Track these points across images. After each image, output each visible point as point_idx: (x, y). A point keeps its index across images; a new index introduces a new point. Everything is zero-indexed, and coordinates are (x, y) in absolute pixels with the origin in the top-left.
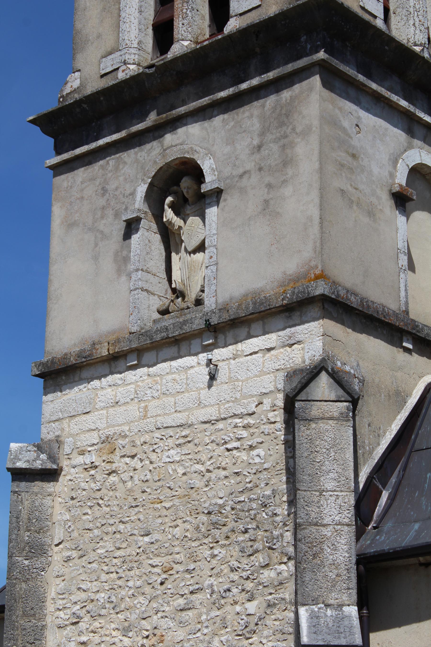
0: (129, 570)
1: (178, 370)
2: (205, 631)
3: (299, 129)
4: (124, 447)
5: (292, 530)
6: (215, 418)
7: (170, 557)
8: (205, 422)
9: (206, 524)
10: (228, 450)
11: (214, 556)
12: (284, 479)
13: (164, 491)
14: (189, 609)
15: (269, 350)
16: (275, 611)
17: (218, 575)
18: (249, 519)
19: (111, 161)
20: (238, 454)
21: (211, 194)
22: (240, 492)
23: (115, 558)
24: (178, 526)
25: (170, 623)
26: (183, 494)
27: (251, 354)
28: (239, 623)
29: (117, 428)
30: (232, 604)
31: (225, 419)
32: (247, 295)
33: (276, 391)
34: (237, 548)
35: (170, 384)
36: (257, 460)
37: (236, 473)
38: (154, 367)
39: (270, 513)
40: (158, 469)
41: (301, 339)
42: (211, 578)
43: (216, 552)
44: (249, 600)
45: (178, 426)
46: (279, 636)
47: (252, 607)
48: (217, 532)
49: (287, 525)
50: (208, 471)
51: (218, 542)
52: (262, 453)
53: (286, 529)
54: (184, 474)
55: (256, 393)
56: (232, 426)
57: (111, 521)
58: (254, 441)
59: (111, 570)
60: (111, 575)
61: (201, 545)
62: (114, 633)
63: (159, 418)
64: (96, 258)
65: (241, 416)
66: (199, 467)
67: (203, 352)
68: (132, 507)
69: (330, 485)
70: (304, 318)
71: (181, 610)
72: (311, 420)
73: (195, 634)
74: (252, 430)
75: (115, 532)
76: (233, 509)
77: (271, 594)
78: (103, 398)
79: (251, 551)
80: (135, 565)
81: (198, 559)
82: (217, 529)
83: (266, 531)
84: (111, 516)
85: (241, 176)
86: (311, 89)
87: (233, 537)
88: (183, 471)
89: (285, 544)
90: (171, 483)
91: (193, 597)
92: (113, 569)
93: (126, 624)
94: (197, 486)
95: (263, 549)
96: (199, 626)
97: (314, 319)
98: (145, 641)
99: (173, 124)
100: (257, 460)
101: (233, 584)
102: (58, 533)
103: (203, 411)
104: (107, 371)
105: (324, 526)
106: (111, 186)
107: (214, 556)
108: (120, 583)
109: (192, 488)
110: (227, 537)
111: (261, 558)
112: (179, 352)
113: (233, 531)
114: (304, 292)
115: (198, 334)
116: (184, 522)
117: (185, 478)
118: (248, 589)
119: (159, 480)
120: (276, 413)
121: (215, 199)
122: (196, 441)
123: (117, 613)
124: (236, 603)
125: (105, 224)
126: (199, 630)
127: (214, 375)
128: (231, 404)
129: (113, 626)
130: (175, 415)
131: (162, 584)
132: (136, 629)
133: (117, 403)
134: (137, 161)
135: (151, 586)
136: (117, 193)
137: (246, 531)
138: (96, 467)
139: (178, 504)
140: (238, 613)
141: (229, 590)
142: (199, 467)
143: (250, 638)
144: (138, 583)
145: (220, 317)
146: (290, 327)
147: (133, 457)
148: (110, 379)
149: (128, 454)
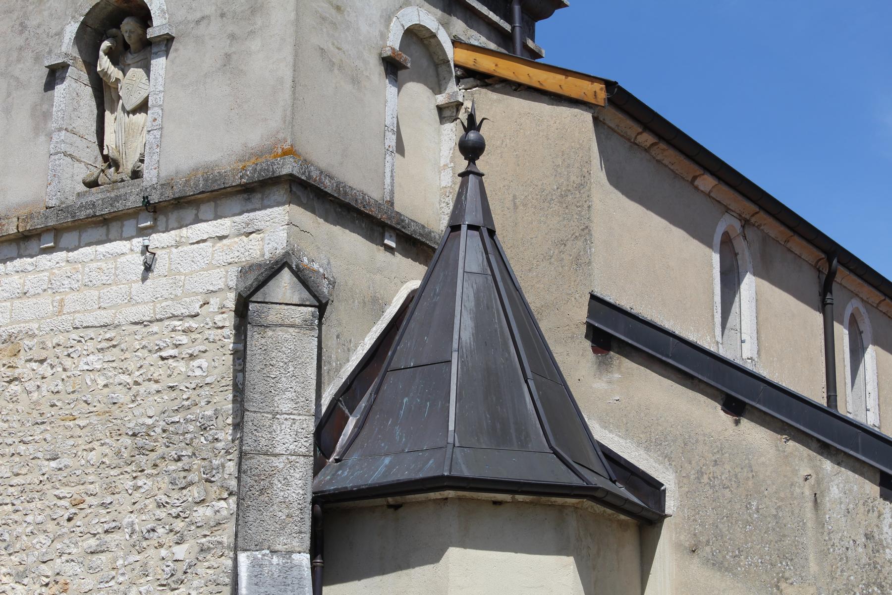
0: (28, 502)
2: (121, 579)
4: (30, 349)
5: (236, 460)
6: (148, 319)
7: (81, 487)
8: (136, 323)
9: (129, 448)
10: (163, 359)
11: (137, 488)
12: (231, 397)
13: (80, 406)
14: (102, 552)
15: (221, 238)
16: (209, 557)
17: (141, 511)
18: (183, 444)
20: (175, 364)
21: (160, 41)
22: (174, 411)
23: (12, 486)
24: (94, 449)
25: (77, 568)
26: (103, 410)
27: (198, 242)
28: (163, 571)
29: (22, 325)
30: (156, 548)
31: (161, 320)
32: (197, 169)
33: (227, 289)
34: (167, 479)
35: (94, 274)
36: (198, 372)
37: (171, 387)
38: (76, 252)
39: (210, 438)
40: (73, 378)
41: (261, 227)
42: (132, 515)
43: (140, 483)
44: (177, 543)
45: (101, 326)
47: (180, 551)
48: (143, 459)
49: (230, 454)
50: (136, 383)
51: (143, 471)
53: (228, 457)
54: (106, 386)
55: (201, 290)
56: (170, 329)
57: (10, 441)
58: (195, 350)
59: (5, 502)
60: (5, 507)
61: (122, 474)
62: (5, 580)
63: (77, 315)
65: (181, 318)
66: (125, 378)
67: (138, 236)
68: (37, 423)
69: (286, 406)
70: (266, 202)
71: (92, 553)
72: (267, 327)
73: (107, 582)
74: (193, 336)
75: (13, 454)
76: (164, 431)
77: (205, 536)
80: (37, 495)
81: (117, 490)
82: (143, 454)
83: (204, 459)
84: (10, 434)
85: (198, 22)
87: (162, 465)
88: (105, 382)
89: (226, 477)
90: (89, 396)
92: (8, 500)
93: (21, 568)
94: (121, 401)
95: (199, 481)
96: (113, 573)
97: (279, 204)
98: (44, 589)
100: (198, 372)
101: (159, 522)
103: (134, 309)
104: (15, 254)
105: (276, 455)
106: (32, 22)
107: (137, 488)
108: (15, 517)
109: (114, 403)
110: (156, 465)
111: (195, 493)
112: (107, 235)
113: (164, 458)
114: (268, 170)
115: (133, 214)
116: (102, 445)
117: (106, 390)
118: (178, 529)
119: (73, 392)
120: (225, 316)
121: (163, 48)
122: (123, 346)
123: (10, 554)
124: (161, 546)
125: (22, 69)
126: (113, 578)
127: (150, 266)
128: (169, 303)
129: (4, 570)
130: (98, 312)
131: (69, 520)
132: (33, 575)
133: (25, 293)
135: (56, 522)
136: (40, 31)
137: (179, 459)
139: (96, 422)
140: (163, 559)
141: (153, 530)
142: (125, 378)
143: (176, 589)
144: (40, 519)
145: (162, 194)
146: (248, 211)
147: (42, 362)
148: (18, 263)
149: (36, 358)
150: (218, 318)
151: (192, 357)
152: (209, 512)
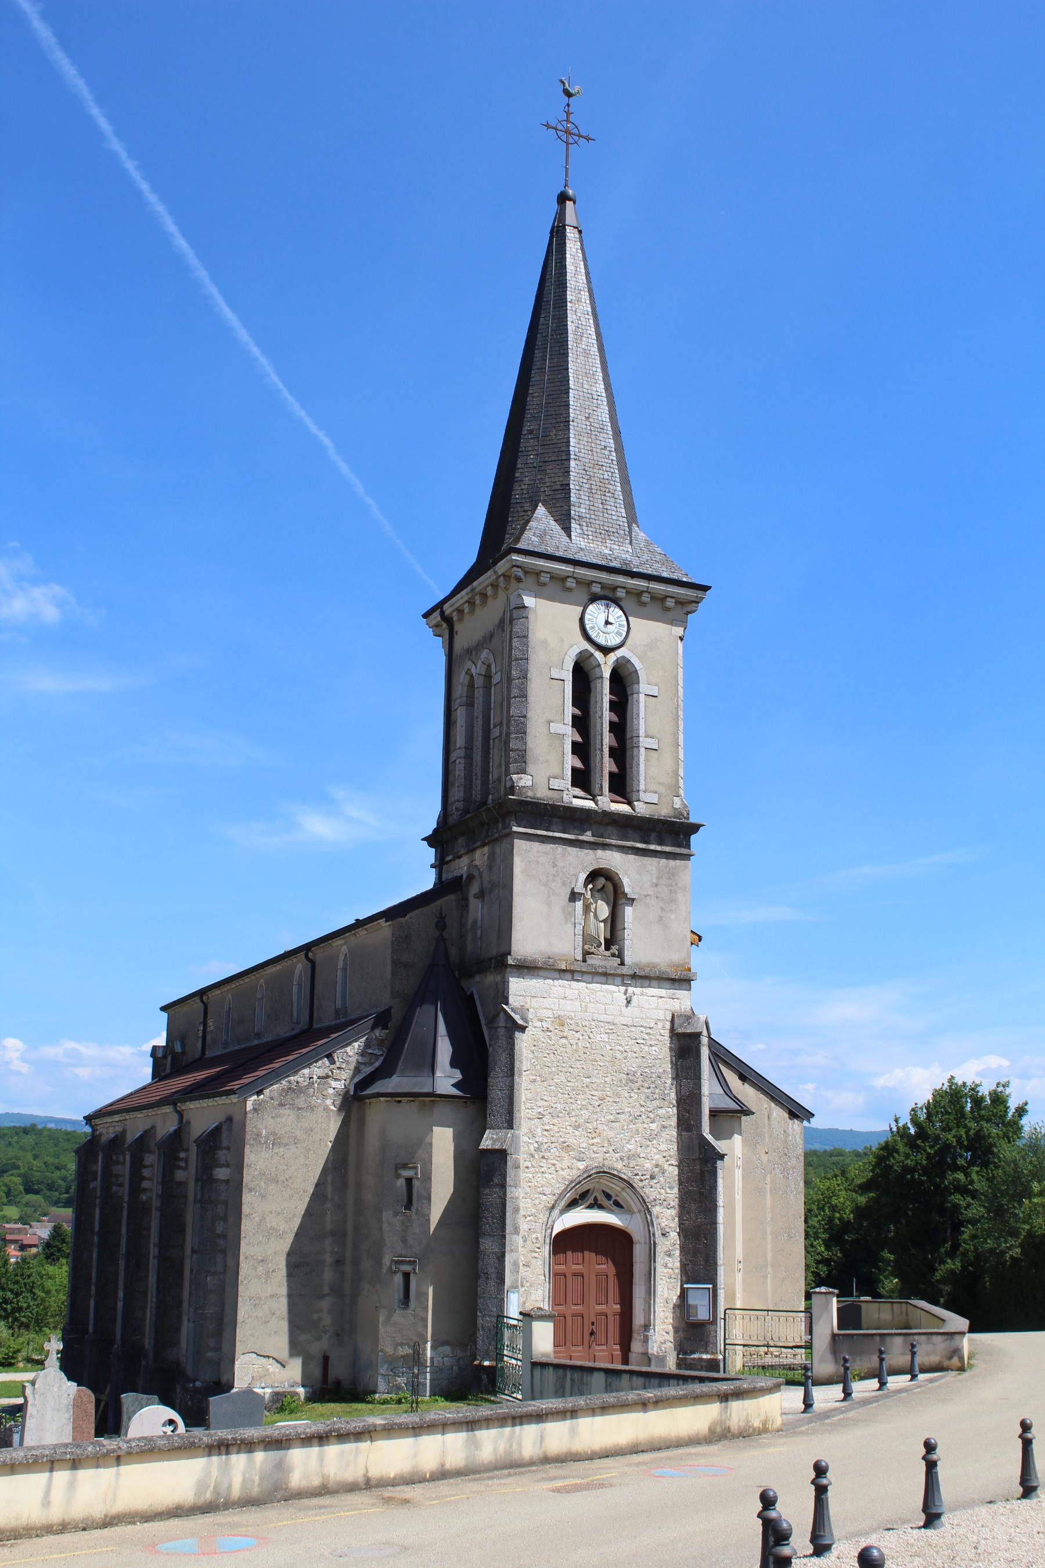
1: (606, 991)
19: (560, 848)
47: (653, 1126)
48: (633, 1086)
58: (653, 1043)
65: (646, 1027)
85: (646, 896)
99: (605, 846)
106: (560, 864)
111: (656, 1103)
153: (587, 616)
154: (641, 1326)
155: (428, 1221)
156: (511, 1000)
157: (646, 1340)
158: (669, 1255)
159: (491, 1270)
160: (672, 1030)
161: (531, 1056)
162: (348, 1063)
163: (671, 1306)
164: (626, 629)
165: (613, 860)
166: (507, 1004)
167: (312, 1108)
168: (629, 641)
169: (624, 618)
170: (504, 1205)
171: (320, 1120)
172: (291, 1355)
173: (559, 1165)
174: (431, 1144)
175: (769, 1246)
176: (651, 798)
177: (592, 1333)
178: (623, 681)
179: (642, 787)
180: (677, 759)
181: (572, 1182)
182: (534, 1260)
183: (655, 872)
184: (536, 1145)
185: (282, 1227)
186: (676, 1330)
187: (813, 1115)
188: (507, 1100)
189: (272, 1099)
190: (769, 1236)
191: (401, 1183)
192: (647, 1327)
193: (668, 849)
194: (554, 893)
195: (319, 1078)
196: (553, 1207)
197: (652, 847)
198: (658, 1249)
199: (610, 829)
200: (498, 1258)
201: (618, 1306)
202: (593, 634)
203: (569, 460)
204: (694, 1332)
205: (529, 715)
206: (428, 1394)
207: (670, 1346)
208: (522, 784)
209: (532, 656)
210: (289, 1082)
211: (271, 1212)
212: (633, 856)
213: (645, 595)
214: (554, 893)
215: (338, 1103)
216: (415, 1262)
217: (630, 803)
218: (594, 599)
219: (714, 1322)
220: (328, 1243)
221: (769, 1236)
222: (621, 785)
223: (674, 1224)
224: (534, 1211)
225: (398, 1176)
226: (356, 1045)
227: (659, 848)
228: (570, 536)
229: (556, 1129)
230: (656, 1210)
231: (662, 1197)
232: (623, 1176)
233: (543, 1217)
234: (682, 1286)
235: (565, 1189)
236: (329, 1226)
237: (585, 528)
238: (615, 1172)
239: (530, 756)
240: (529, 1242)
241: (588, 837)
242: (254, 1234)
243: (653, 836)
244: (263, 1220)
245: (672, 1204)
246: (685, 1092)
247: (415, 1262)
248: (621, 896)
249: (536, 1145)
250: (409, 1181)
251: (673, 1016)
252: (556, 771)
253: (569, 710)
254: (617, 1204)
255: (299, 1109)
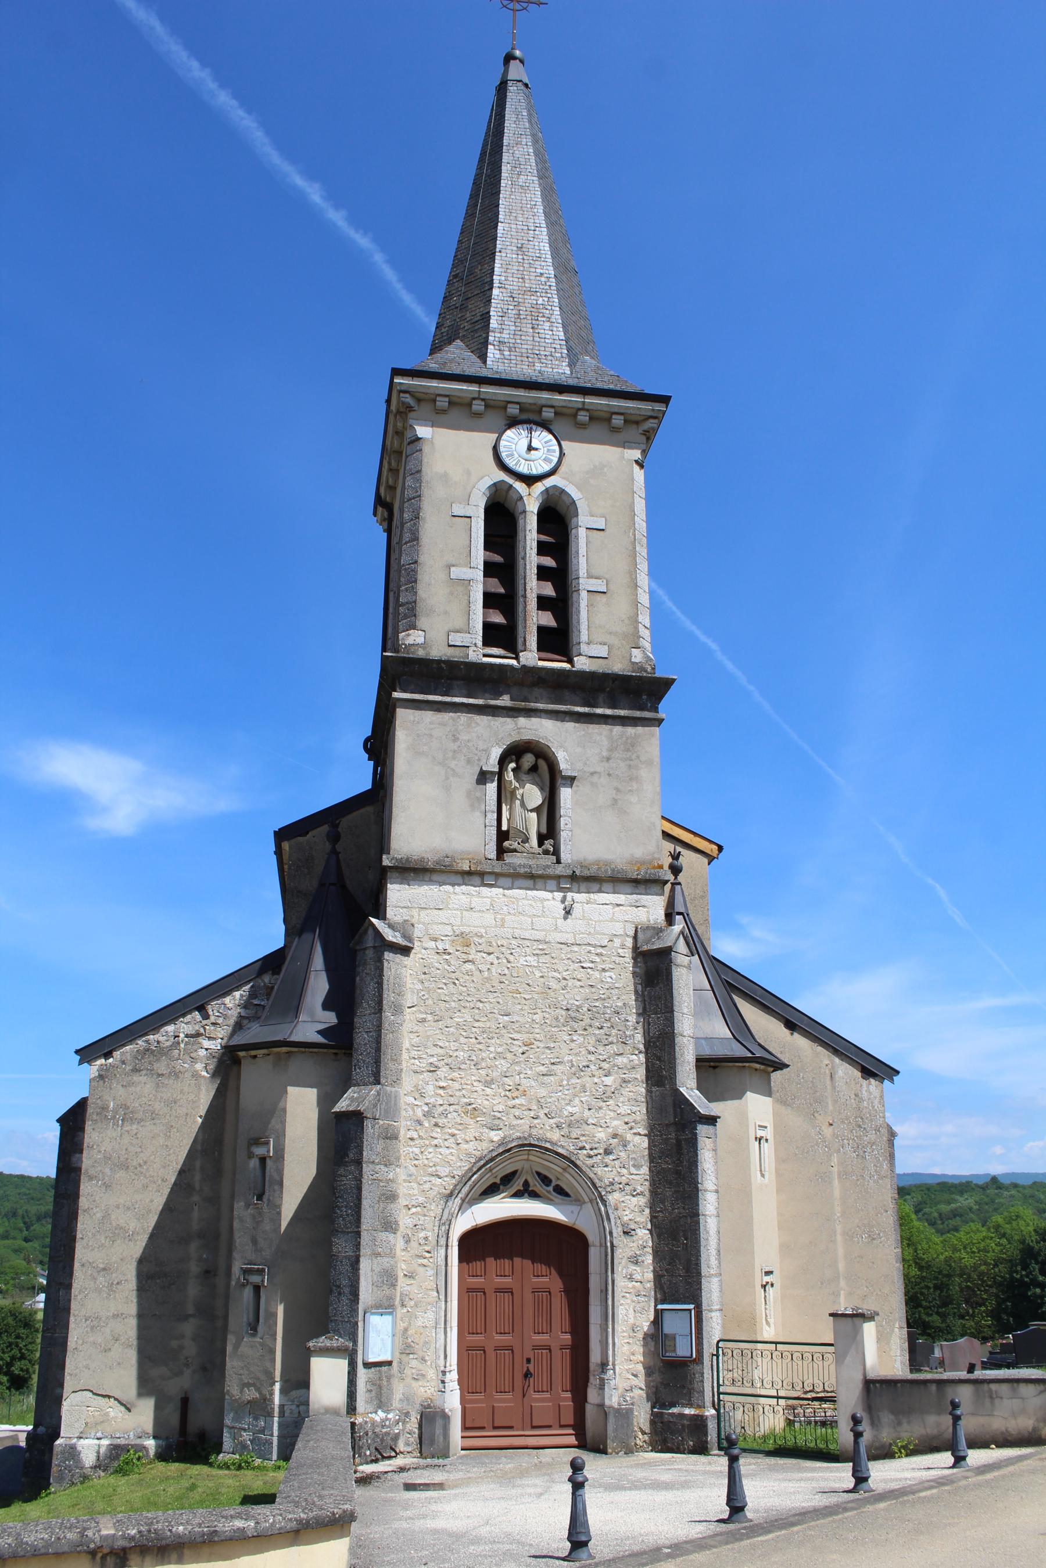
3: (643, 759)
11: (573, 1041)
15: (618, 905)
17: (577, 1054)
19: (463, 718)
36: (609, 980)
46: (633, 1103)
47: (608, 1080)
48: (575, 1025)
50: (565, 979)
52: (614, 977)
57: (469, 999)
58: (607, 966)
62: (475, 1084)
64: (447, 789)
65: (595, 946)
66: (556, 974)
69: (685, 1011)
78: (456, 901)
79: (606, 1042)
85: (592, 774)
86: (652, 735)
91: (554, 1067)
97: (657, 894)
99: (530, 713)
100: (609, 980)
102: (409, 999)
106: (464, 737)
107: (573, 1041)
108: (480, 1046)
115: (558, 878)
129: (473, 1078)
131: (523, 1053)
134: (489, 726)
137: (602, 1028)
138: (450, 954)
142: (556, 974)
144: (499, 1050)
147: (489, 954)
148: (463, 887)
150: (620, 951)
151: (603, 969)
152: (625, 1060)
153: (502, 443)
154: (597, 1365)
155: (279, 1214)
156: (390, 913)
157: (602, 1387)
158: (636, 1263)
159: (345, 1282)
160: (635, 948)
161: (420, 986)
162: (225, 1017)
163: (640, 1336)
164: (557, 454)
165: (542, 729)
166: (381, 915)
167: (176, 1074)
168: (563, 469)
169: (554, 442)
170: (359, 1189)
171: (186, 1089)
172: (140, 1395)
173: (461, 1136)
174: (284, 1110)
175: (840, 1251)
176: (596, 648)
177: (527, 1375)
178: (556, 518)
179: (584, 637)
180: (636, 603)
181: (480, 1159)
182: (421, 1269)
183: (605, 743)
184: (426, 1108)
185: (133, 1225)
186: (649, 1372)
187: (898, 1072)
188: (374, 1045)
189: (123, 1062)
190: (839, 1238)
191: (254, 1163)
192: (604, 1365)
193: (622, 713)
194: (455, 774)
195: (187, 1036)
196: (451, 1195)
197: (599, 711)
198: (619, 1253)
199: (537, 691)
200: (351, 1265)
201: (568, 1336)
202: (511, 463)
203: (491, 289)
204: (673, 1373)
205: (421, 559)
206: (275, 1457)
207: (639, 1394)
208: (410, 641)
209: (426, 492)
210: (147, 1041)
211: (118, 1207)
212: (573, 724)
213: (582, 413)
214: (455, 774)
215: (211, 1067)
216: (263, 1270)
217: (570, 661)
218: (513, 423)
219: (699, 1360)
220: (193, 1247)
221: (839, 1238)
222: (557, 640)
223: (644, 1217)
224: (421, 1199)
225: (251, 1155)
226: (237, 994)
227: (609, 712)
228: (485, 362)
229: (457, 1085)
230: (613, 1198)
231: (624, 1180)
232: (560, 1150)
233: (435, 1209)
234: (656, 1306)
235: (470, 1169)
236: (195, 1226)
237: (507, 353)
238: (548, 1145)
239: (420, 607)
240: (414, 1244)
241: (505, 701)
242: (94, 1235)
243: (601, 698)
244: (106, 1216)
245: (639, 1189)
246: (654, 1031)
247: (263, 1270)
248: (558, 776)
249: (426, 1108)
250: (263, 1160)
251: (637, 928)
252: (459, 622)
253: (479, 555)
254: (560, 1191)
255: (159, 1075)
